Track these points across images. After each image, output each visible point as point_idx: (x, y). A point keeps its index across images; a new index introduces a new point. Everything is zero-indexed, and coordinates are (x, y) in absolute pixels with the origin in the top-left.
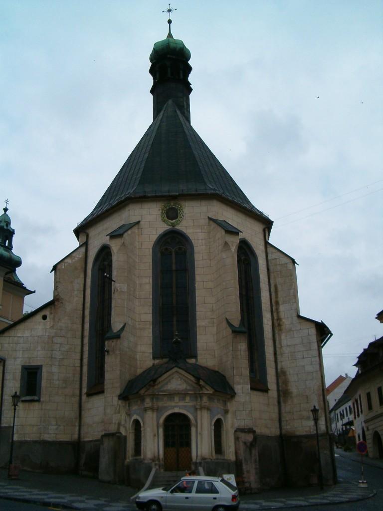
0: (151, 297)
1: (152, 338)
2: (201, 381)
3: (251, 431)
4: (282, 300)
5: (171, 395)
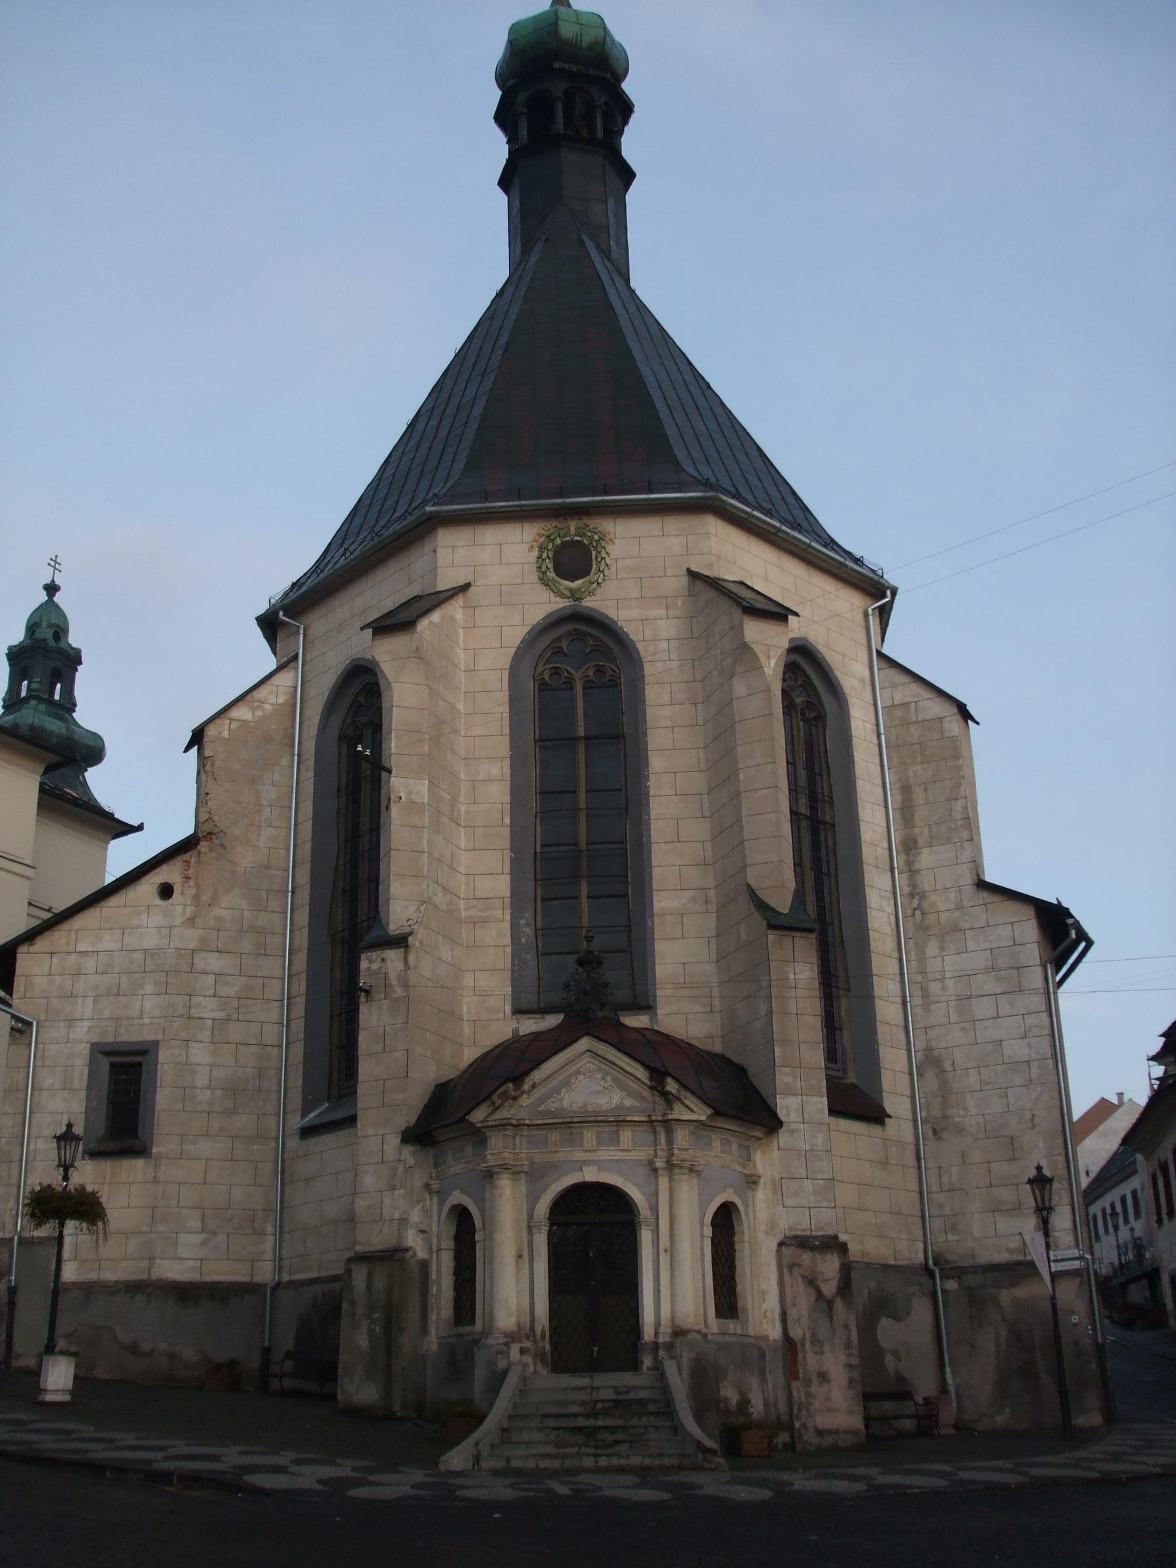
0: (507, 821)
1: (509, 950)
2: (669, 1080)
3: (832, 1244)
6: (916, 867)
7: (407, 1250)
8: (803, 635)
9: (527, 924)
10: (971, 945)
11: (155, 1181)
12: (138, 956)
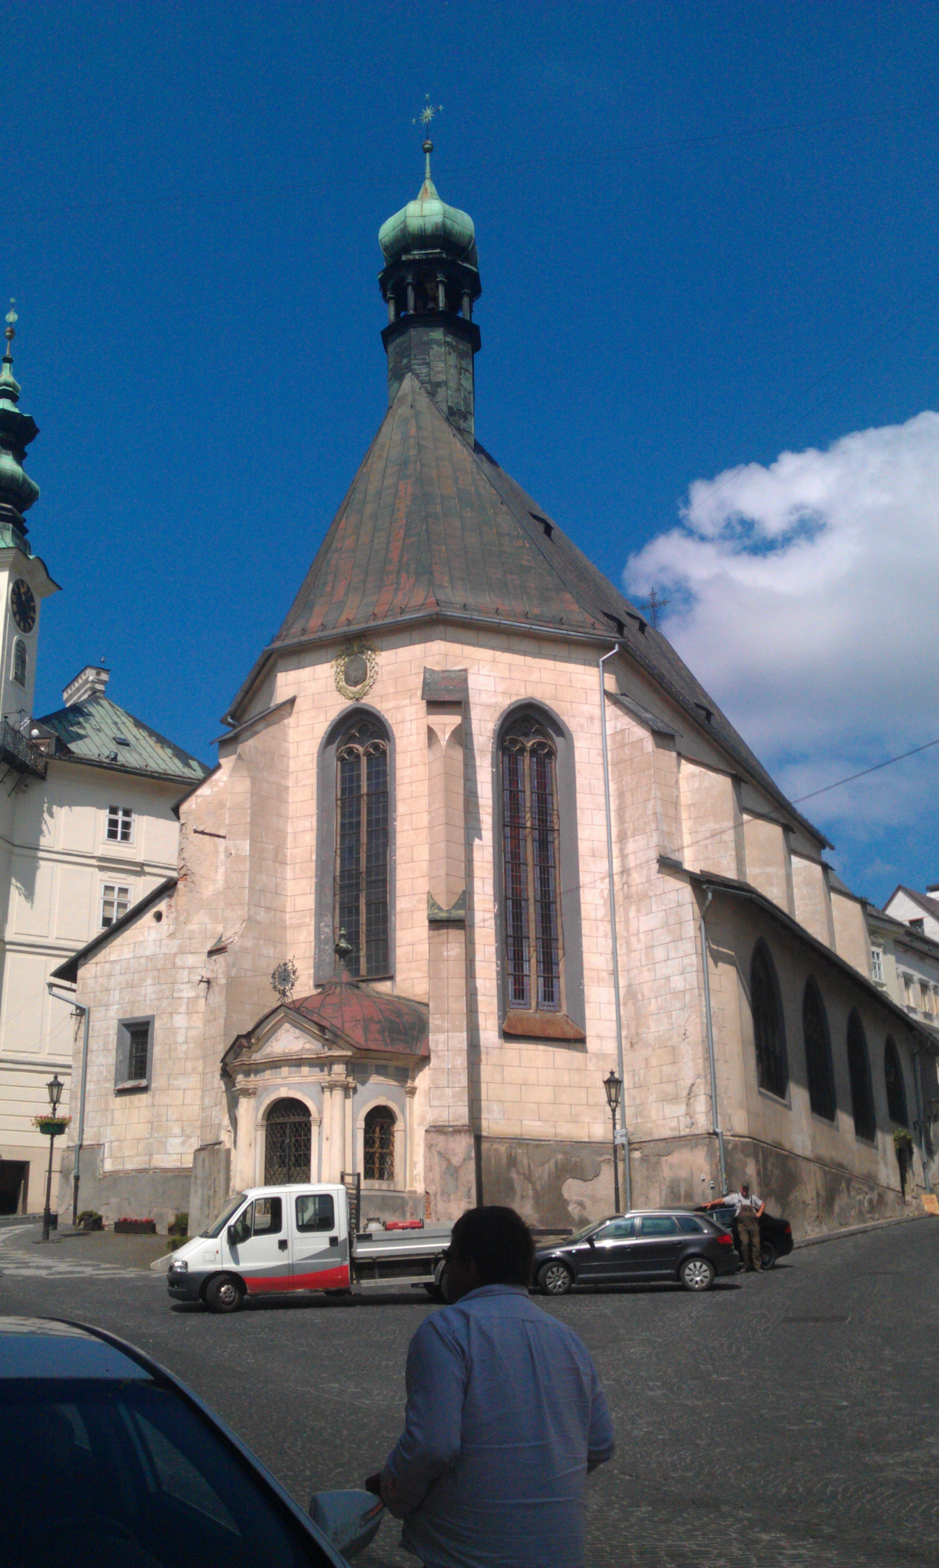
0: (314, 858)
1: (313, 944)
4: (631, 827)
5: (275, 1064)
6: (626, 852)
7: (220, 1143)
9: (327, 926)
10: (654, 908)
11: (153, 1105)
12: (143, 960)
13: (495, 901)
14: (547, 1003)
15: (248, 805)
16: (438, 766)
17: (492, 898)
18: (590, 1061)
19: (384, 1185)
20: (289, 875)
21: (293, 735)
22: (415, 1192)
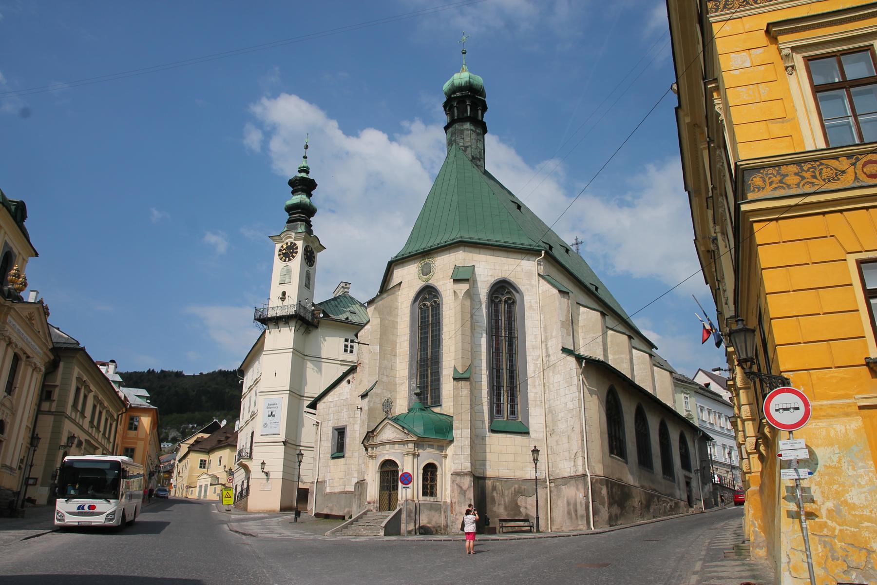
0: (408, 353)
5: (383, 444)
6: (548, 346)
8: (503, 276)
11: (346, 464)
12: (342, 401)
13: (487, 370)
14: (512, 416)
15: (379, 330)
16: (459, 308)
17: (486, 368)
18: (531, 442)
19: (432, 499)
20: (398, 361)
21: (400, 299)
22: (447, 502)
